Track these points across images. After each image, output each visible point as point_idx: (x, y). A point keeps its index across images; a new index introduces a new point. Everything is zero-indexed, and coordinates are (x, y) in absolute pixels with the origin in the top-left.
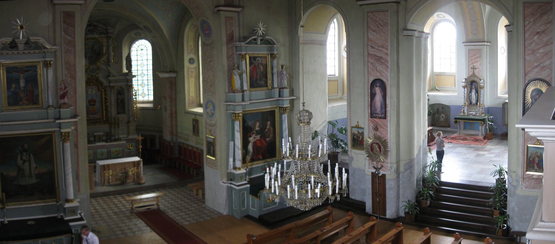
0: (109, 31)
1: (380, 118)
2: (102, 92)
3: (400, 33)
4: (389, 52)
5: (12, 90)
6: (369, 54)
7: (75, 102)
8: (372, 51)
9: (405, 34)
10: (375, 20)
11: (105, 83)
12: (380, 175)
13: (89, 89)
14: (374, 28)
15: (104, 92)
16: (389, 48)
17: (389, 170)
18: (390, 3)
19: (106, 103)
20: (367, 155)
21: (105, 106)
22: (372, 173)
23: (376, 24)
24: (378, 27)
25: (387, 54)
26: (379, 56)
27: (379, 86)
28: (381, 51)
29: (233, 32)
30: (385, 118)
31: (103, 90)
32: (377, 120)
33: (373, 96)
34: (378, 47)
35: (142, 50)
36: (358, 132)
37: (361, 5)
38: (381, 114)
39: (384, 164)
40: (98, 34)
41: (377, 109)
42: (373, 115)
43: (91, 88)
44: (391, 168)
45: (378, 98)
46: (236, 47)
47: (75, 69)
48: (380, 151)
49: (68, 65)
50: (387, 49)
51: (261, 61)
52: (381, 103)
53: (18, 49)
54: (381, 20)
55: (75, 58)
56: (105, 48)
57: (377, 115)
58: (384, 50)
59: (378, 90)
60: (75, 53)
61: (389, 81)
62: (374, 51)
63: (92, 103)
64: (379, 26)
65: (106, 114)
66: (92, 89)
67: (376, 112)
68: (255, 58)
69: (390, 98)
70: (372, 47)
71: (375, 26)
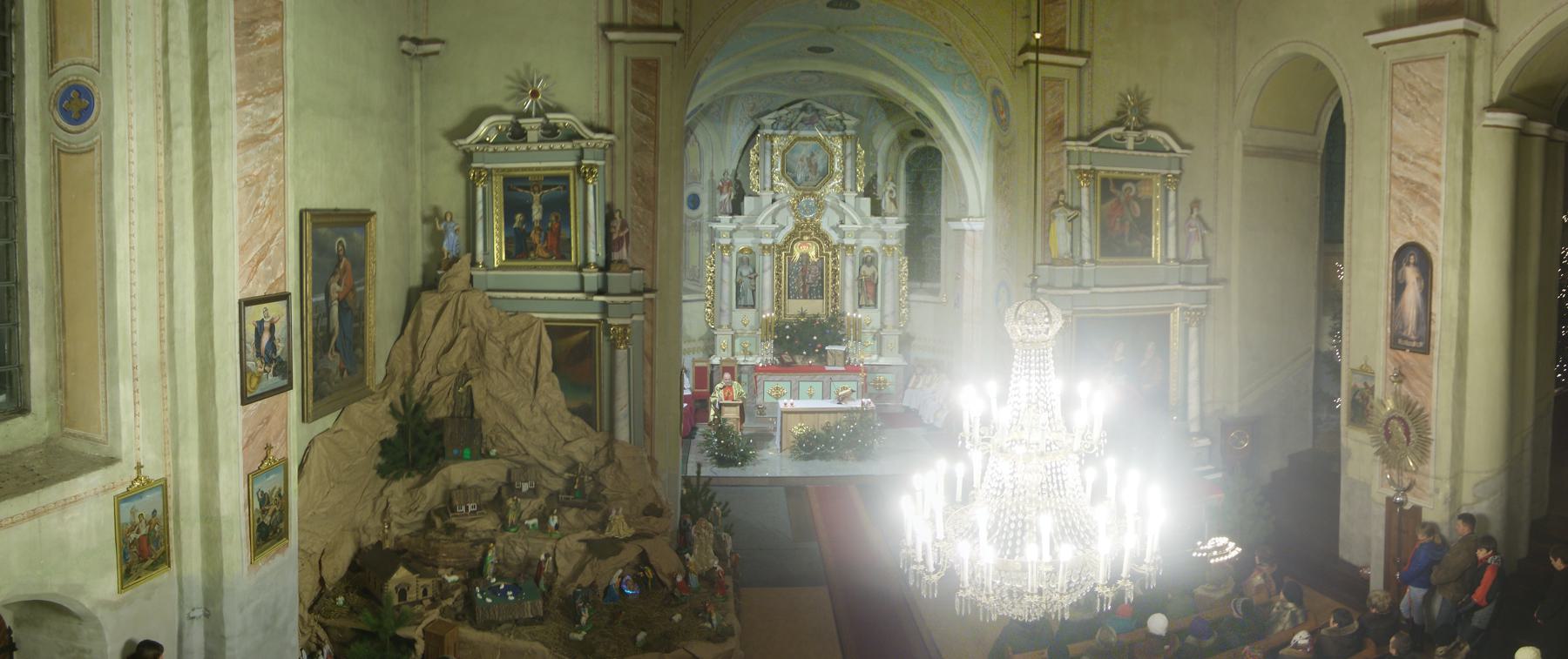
0: (845, 122)
1: (1414, 350)
2: (827, 256)
3: (1475, 121)
4: (1442, 170)
5: (516, 225)
6: (1393, 176)
7: (653, 261)
8: (1400, 169)
9: (1487, 122)
10: (1410, 85)
11: (834, 238)
12: (1408, 507)
14: (1408, 107)
15: (832, 257)
16: (1443, 160)
17: (1431, 496)
18: (1449, 37)
19: (834, 281)
20: (1375, 449)
22: (1389, 499)
23: (1412, 95)
24: (1418, 103)
25: (1437, 176)
26: (1417, 183)
27: (1415, 264)
28: (1424, 168)
29: (1061, 115)
30: (1426, 350)
31: (830, 253)
32: (1406, 355)
33: (1399, 288)
34: (1414, 157)
36: (1365, 384)
37: (1377, 46)
38: (1418, 341)
39: (1418, 479)
41: (1408, 327)
42: (1396, 341)
44: (1437, 491)
45: (1412, 295)
46: (1068, 152)
47: (655, 188)
48: (1408, 440)
49: (639, 179)
50: (1438, 163)
51: (1137, 190)
52: (1418, 309)
53: (526, 142)
54: (1425, 83)
55: (656, 163)
57: (1407, 343)
58: (1432, 167)
59: (1411, 275)
60: (656, 153)
61: (1441, 251)
62: (1406, 168)
64: (1419, 100)
67: (1404, 334)
68: (1119, 182)
69: (1442, 297)
70: (1400, 157)
71: (1409, 101)
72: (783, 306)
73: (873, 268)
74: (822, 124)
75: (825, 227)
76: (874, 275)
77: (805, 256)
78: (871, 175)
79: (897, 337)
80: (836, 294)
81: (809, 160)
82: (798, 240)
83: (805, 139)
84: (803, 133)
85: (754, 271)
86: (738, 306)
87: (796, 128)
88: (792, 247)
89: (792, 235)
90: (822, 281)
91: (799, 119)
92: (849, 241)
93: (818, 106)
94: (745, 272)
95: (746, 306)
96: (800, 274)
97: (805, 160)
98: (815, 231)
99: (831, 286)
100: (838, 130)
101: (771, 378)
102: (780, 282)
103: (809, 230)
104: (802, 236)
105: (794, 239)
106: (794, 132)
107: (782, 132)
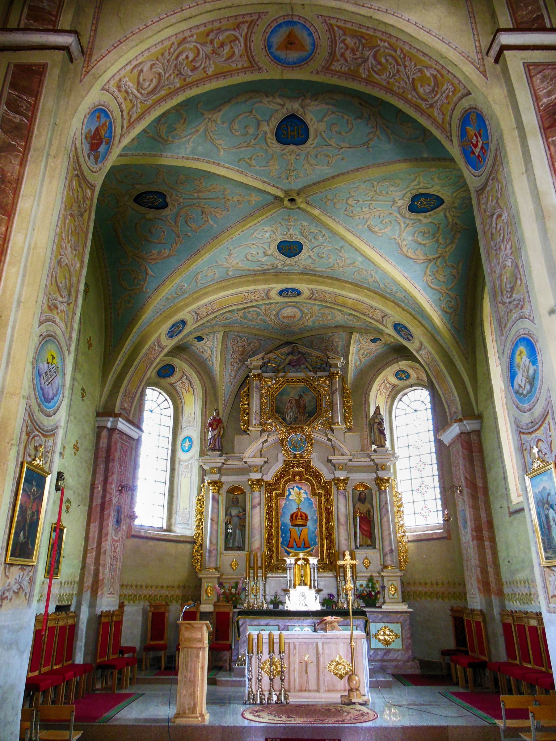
11: (327, 475)
13: (293, 489)
15: (325, 495)
19: (328, 521)
21: (327, 529)
35: (416, 411)
40: (310, 371)
43: (297, 487)
63: (299, 522)
65: (329, 548)
66: (300, 489)
74: (308, 365)
75: (317, 464)
76: (369, 511)
79: (399, 579)
82: (289, 480)
83: (292, 381)
84: (291, 375)
85: (244, 510)
86: (227, 548)
87: (284, 370)
88: (284, 486)
89: (283, 473)
91: (287, 361)
92: (342, 475)
94: (234, 512)
95: (232, 549)
97: (293, 402)
100: (324, 371)
101: (255, 622)
102: (272, 522)
104: (294, 476)
105: (286, 478)
106: (281, 374)
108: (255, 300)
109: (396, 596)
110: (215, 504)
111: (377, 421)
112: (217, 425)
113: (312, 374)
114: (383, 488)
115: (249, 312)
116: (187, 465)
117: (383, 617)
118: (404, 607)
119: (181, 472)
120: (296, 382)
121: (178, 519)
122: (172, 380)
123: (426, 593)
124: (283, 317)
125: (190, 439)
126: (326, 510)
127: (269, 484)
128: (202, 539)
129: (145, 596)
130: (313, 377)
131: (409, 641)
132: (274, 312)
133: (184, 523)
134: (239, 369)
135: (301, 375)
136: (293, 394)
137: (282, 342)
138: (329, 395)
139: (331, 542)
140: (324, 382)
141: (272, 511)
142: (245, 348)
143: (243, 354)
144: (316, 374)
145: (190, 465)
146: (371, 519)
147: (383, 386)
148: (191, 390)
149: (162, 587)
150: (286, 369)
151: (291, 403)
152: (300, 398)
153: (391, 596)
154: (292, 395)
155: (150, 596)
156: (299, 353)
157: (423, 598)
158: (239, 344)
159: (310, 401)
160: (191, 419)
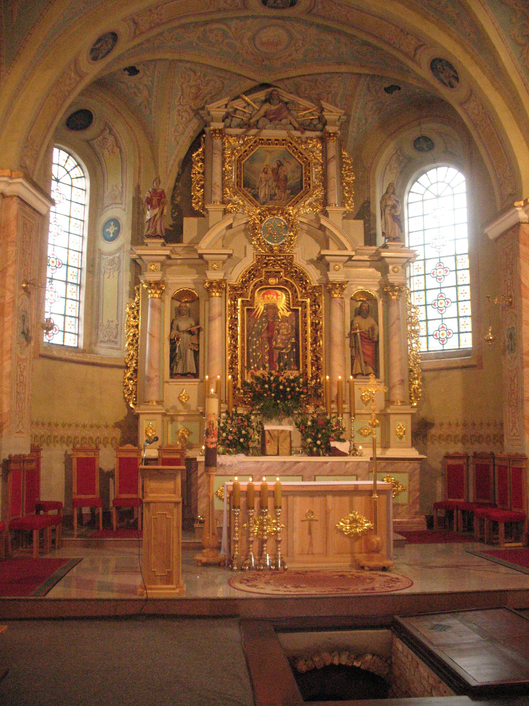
2: (303, 305)
15: (311, 306)
19: (315, 340)
21: (313, 351)
31: (308, 301)
35: (438, 197)
40: (295, 129)
56: (316, 170)
72: (239, 376)
73: (370, 321)
76: (372, 329)
77: (272, 308)
78: (362, 201)
79: (409, 417)
80: (318, 359)
81: (276, 172)
83: (268, 142)
84: (269, 133)
85: (197, 323)
86: (173, 375)
87: (256, 125)
88: (253, 292)
89: (252, 273)
90: (296, 345)
91: (262, 112)
93: (287, 97)
96: (265, 335)
97: (270, 172)
98: (286, 269)
99: (309, 347)
102: (236, 340)
103: (277, 268)
104: (268, 277)
105: (256, 280)
106: (253, 131)
107: (239, 131)
108: (225, 10)
109: (404, 439)
110: (157, 315)
111: (390, 203)
112: (159, 201)
113: (297, 134)
114: (393, 297)
115: (211, 31)
116: (113, 260)
117: (387, 464)
118: (414, 453)
119: (103, 270)
120: (273, 144)
121: (101, 335)
122: (89, 133)
123: (440, 436)
124: (262, 43)
125: (116, 222)
126: (312, 326)
127: (234, 288)
128: (136, 363)
129: (62, 438)
130: (299, 138)
131: (418, 494)
132: (250, 34)
133: (109, 341)
134: (190, 121)
135: (281, 134)
136: (270, 162)
137: (253, 84)
138: (322, 165)
139: (318, 369)
140: (314, 146)
141: (236, 325)
142: (199, 89)
143: (196, 97)
144: (302, 133)
145: (116, 259)
146: (375, 339)
147: (394, 158)
148: (117, 150)
149: (84, 426)
150: (260, 124)
151: (266, 173)
152: (279, 166)
153: (398, 439)
154: (267, 162)
155: (69, 437)
156: (281, 101)
157: (436, 442)
158: (192, 83)
159: (293, 172)
160: (116, 193)
